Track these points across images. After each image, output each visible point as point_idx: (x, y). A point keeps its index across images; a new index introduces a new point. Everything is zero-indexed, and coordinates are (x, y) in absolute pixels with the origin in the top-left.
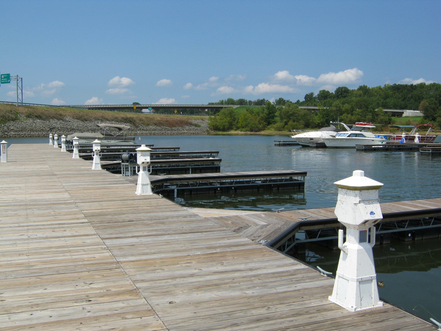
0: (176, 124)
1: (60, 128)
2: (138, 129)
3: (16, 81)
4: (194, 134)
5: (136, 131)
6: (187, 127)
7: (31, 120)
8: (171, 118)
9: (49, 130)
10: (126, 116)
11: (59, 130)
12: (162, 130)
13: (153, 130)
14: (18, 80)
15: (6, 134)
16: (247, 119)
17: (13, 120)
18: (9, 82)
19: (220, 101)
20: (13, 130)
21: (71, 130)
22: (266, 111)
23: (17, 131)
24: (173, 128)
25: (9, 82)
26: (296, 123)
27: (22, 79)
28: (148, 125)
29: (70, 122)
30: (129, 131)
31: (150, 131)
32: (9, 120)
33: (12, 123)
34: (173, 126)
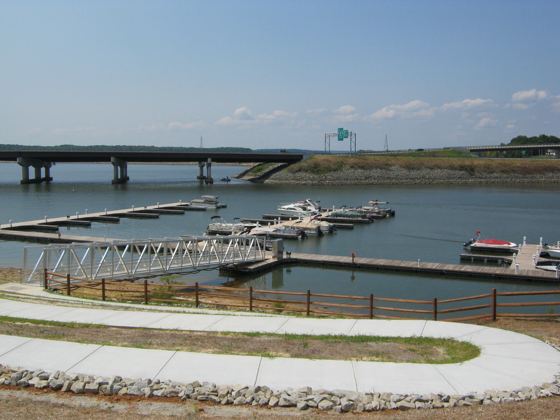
0: (535, 170)
2: (473, 177)
4: (554, 182)
5: (468, 179)
6: (551, 174)
7: (352, 170)
8: (537, 164)
10: (472, 163)
13: (494, 178)
14: (351, 136)
15: (321, 183)
17: (335, 170)
18: (347, 137)
24: (527, 176)
25: (347, 137)
27: (355, 134)
28: (491, 172)
30: (459, 179)
32: (330, 171)
33: (332, 173)
34: (528, 173)
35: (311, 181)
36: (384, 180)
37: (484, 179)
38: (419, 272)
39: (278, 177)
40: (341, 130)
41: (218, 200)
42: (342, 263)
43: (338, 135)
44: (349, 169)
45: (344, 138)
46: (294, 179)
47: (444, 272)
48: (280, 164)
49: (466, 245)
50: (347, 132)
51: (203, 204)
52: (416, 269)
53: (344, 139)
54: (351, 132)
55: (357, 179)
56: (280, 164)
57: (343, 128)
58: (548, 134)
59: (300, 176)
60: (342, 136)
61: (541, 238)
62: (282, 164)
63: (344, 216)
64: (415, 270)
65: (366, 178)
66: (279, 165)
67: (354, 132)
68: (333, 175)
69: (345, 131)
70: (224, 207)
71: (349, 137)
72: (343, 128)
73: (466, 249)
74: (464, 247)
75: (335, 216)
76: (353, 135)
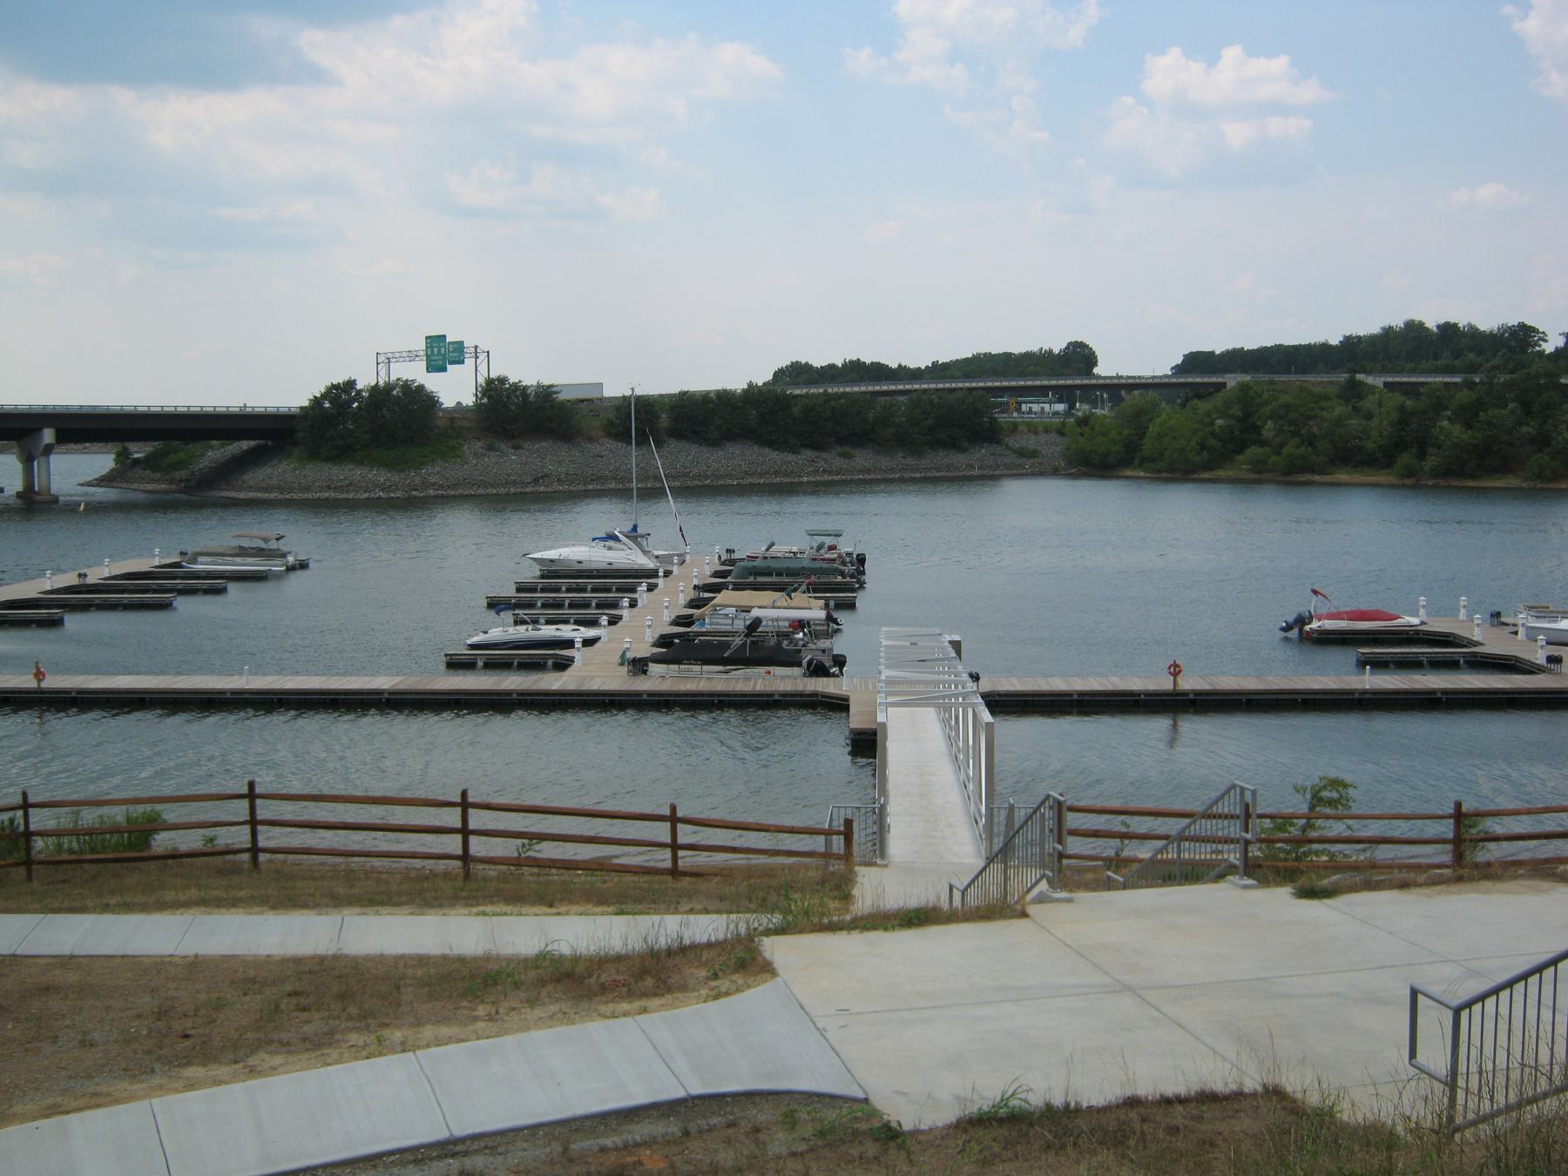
1: (563, 476)
3: (474, 359)
9: (530, 483)
11: (558, 480)
12: (891, 469)
13: (859, 471)
16: (1166, 435)
18: (462, 362)
19: (1383, 329)
20: (434, 484)
21: (593, 480)
22: (1236, 410)
23: (441, 487)
25: (462, 362)
26: (1303, 449)
27: (488, 352)
29: (602, 457)
30: (776, 477)
31: (848, 475)
35: (383, 490)
36: (585, 484)
37: (838, 474)
38: (1368, 700)
39: (275, 482)
40: (436, 342)
41: (282, 546)
42: (1139, 695)
43: (427, 355)
44: (484, 455)
45: (450, 364)
46: (329, 487)
47: (1439, 695)
48: (245, 445)
49: (1288, 628)
50: (459, 347)
51: (238, 560)
52: (1360, 694)
53: (448, 366)
54: (476, 347)
55: (514, 483)
56: (245, 445)
57: (444, 336)
58: (867, 359)
59: (346, 478)
60: (444, 360)
61: (1422, 598)
62: (253, 443)
63: (779, 574)
64: (1357, 696)
65: (536, 481)
66: (245, 448)
67: (482, 347)
68: (443, 472)
69: (456, 343)
70: (303, 566)
71: (470, 362)
72: (444, 336)
73: (1286, 639)
74: (1283, 634)
75: (750, 574)
76: (482, 357)
